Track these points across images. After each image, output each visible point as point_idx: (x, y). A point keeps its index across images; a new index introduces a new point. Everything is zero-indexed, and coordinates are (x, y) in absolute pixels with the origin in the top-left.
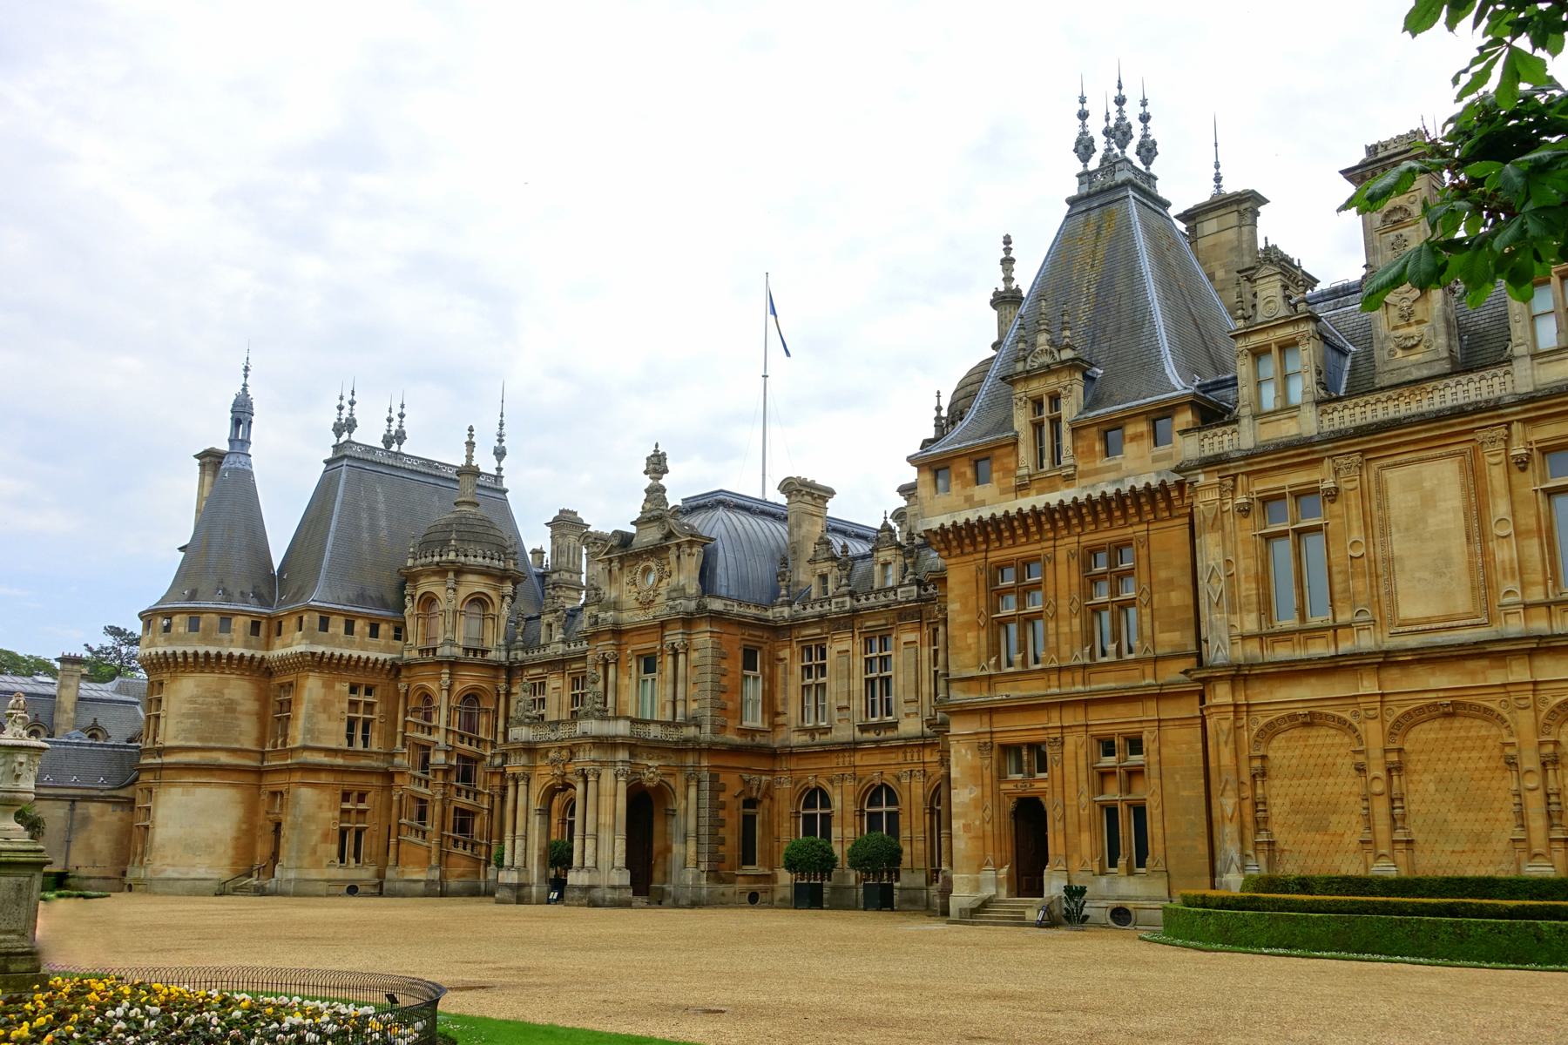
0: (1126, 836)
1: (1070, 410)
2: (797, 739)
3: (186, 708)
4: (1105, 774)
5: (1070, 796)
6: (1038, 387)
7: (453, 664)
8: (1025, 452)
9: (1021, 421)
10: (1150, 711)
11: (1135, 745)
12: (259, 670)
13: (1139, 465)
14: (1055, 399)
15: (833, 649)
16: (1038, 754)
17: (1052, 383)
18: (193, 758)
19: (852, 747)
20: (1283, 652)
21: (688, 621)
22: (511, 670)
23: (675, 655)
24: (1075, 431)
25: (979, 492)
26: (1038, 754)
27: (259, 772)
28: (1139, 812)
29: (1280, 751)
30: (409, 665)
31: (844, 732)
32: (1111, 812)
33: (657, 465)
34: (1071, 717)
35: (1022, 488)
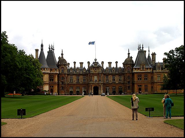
0: (146, 90)
1: (144, 67)
2: (106, 83)
3: (46, 78)
4: (145, 87)
5: (143, 87)
6: (142, 65)
7: (65, 74)
8: (141, 68)
9: (141, 67)
10: (148, 84)
11: (147, 85)
12: (49, 74)
13: (149, 71)
14: (143, 66)
15: (109, 76)
16: (141, 86)
17: (143, 65)
18: (47, 83)
19: (112, 84)
20: (158, 82)
21: (101, 74)
22: (68, 75)
23: (100, 76)
24: (145, 68)
25: (138, 70)
26: (141, 86)
27: (49, 84)
28: (147, 89)
29: (158, 86)
30: (61, 74)
31: (110, 83)
32: (145, 89)
33: (96, 60)
34: (143, 84)
35: (141, 71)
